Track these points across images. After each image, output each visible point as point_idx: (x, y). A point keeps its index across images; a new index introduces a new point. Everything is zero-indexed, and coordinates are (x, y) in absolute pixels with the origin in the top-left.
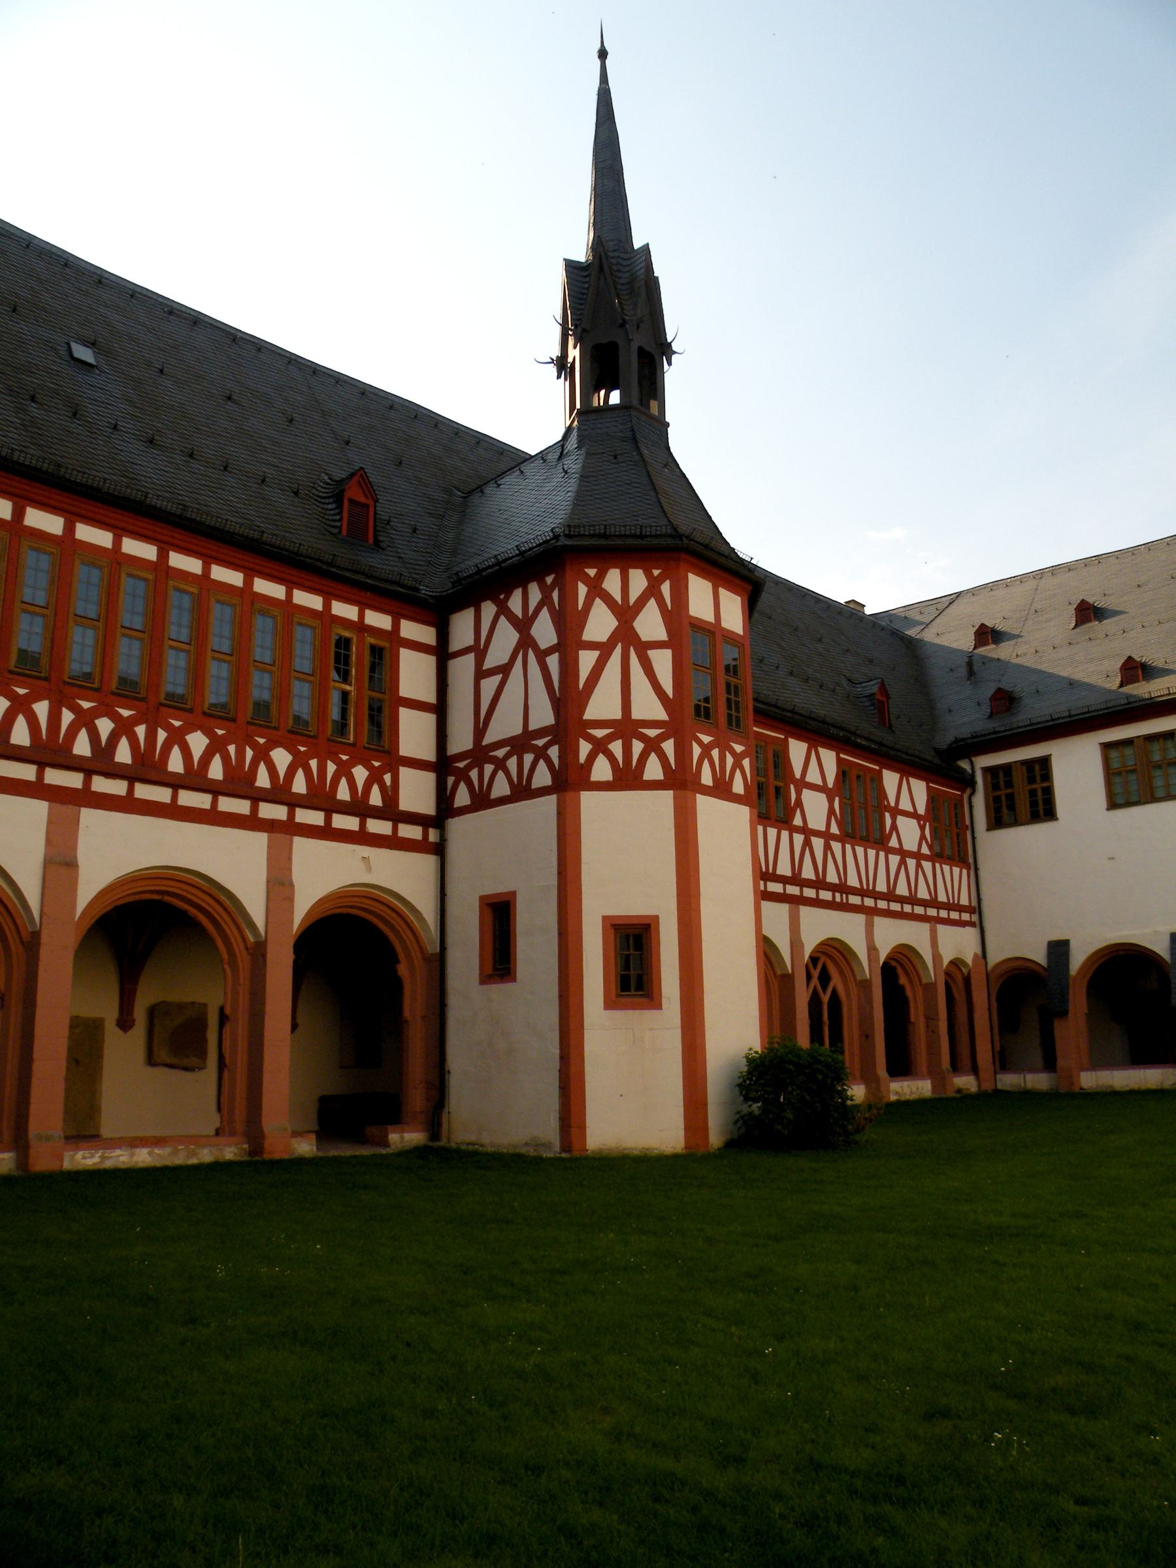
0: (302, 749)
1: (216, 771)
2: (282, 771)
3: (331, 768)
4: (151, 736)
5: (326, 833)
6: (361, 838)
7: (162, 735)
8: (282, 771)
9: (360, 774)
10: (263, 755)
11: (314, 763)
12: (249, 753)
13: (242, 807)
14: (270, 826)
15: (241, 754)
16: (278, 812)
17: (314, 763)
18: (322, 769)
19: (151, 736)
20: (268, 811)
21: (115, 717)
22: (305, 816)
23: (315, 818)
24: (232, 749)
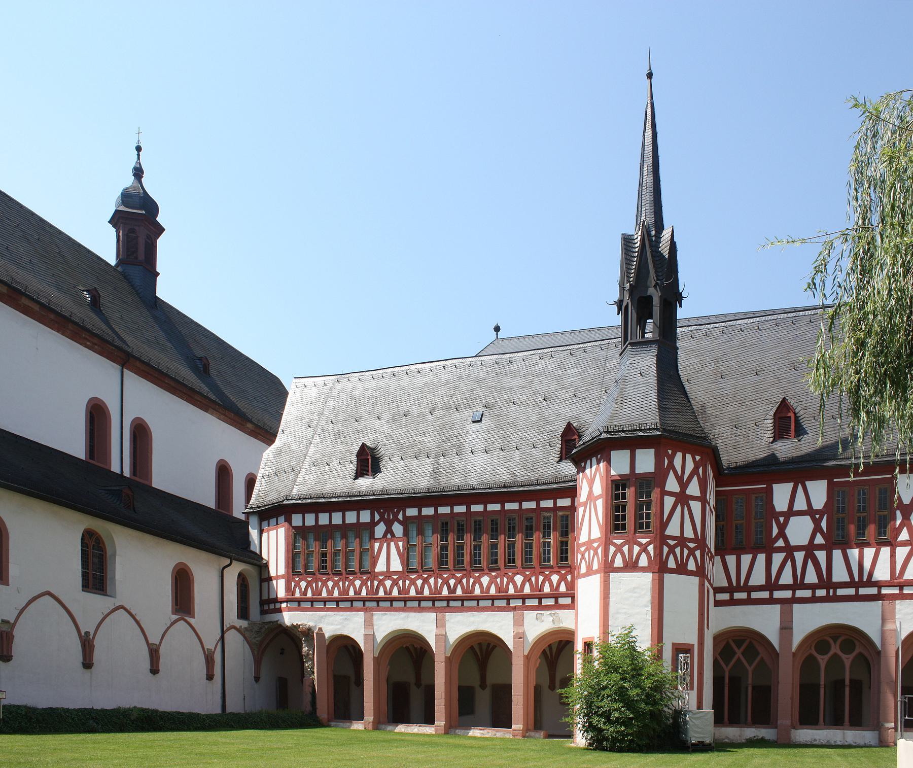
0: (528, 573)
1: (493, 591)
2: (519, 584)
3: (541, 578)
4: (468, 581)
5: (540, 607)
6: (557, 606)
7: (472, 580)
8: (519, 584)
9: (555, 578)
10: (511, 580)
11: (533, 579)
12: (505, 580)
13: (503, 603)
14: (515, 609)
15: (502, 581)
16: (519, 603)
17: (533, 579)
18: (537, 580)
19: (468, 581)
20: (513, 603)
21: (456, 578)
22: (529, 602)
23: (535, 602)
24: (498, 580)
